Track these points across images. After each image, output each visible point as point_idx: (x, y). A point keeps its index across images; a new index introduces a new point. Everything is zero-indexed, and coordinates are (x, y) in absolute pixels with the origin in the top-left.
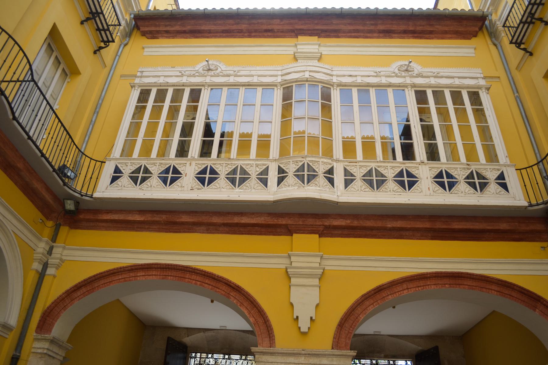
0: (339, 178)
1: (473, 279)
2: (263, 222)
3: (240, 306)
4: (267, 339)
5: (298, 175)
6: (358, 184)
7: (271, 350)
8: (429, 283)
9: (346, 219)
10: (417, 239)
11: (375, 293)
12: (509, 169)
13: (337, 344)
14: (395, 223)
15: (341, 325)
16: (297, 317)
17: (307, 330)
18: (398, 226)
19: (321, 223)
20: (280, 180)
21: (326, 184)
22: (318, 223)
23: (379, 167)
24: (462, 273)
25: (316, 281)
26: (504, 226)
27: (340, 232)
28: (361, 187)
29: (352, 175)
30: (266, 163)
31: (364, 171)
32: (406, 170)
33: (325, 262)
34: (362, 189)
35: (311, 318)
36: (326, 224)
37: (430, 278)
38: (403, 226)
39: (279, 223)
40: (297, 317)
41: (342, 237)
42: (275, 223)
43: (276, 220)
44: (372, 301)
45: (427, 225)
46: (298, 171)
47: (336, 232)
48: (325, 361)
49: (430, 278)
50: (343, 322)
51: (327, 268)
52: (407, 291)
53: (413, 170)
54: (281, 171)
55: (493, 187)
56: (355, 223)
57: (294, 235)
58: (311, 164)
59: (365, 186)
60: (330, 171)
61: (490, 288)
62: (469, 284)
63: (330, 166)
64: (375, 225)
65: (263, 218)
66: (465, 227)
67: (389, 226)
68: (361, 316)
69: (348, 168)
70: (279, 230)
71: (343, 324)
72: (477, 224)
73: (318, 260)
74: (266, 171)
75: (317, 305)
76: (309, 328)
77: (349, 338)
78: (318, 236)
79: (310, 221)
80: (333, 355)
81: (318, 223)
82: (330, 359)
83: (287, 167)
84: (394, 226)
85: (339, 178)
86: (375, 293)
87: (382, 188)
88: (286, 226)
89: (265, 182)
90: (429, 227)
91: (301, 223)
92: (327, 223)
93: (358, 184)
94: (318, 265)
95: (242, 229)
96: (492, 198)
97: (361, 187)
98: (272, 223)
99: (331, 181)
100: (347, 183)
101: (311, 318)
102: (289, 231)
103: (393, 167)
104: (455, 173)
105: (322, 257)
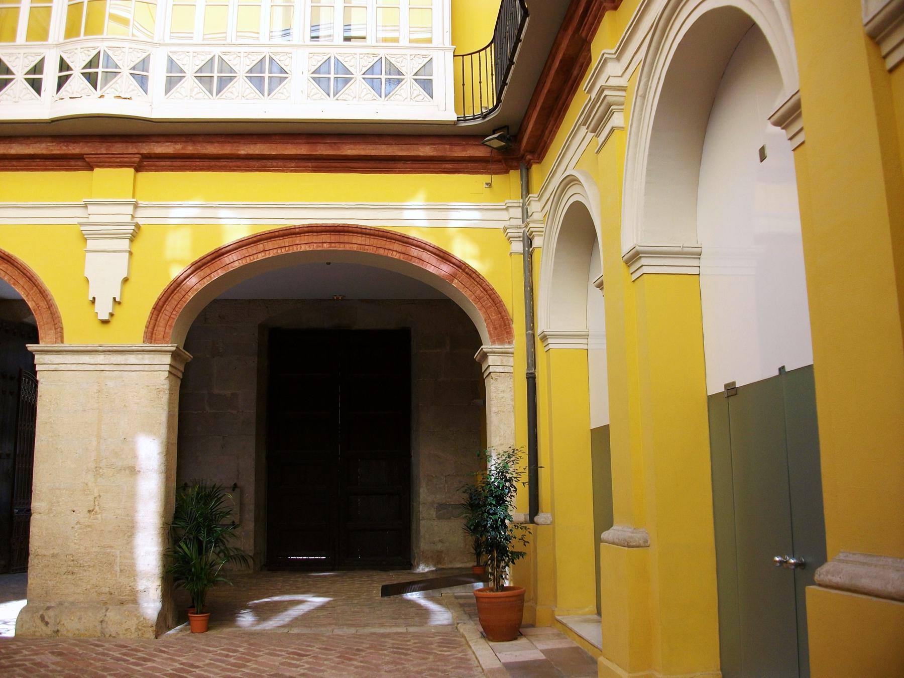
0: (157, 75)
1: (366, 234)
2: (44, 152)
3: (14, 284)
4: (53, 331)
5: (90, 73)
6: (189, 83)
7: (58, 346)
8: (298, 242)
9: (176, 143)
10: (291, 171)
11: (213, 259)
12: (441, 53)
13: (150, 335)
14: (252, 147)
15: (158, 309)
16: (94, 298)
17: (106, 317)
18: (257, 152)
19: (135, 151)
20: (62, 82)
21: (132, 87)
22: (131, 149)
23: (225, 53)
24: (349, 226)
25: (125, 244)
26: (426, 150)
27: (168, 163)
28: (192, 90)
29: (182, 71)
30: (41, 50)
31: (200, 61)
32: (271, 59)
33: (140, 213)
34: (194, 93)
35: (114, 299)
36: (144, 151)
37: (299, 233)
38: (264, 152)
39: (70, 152)
40: (94, 298)
41: (173, 170)
42: (62, 152)
43: (64, 148)
44: (209, 272)
45: (302, 150)
46: (90, 65)
47: (163, 163)
48: (132, 359)
49: (299, 233)
50: (161, 303)
51: (140, 221)
52: (263, 254)
53: (282, 59)
54: (64, 66)
55: (409, 87)
56: (190, 149)
57: (96, 170)
58: (110, 53)
59: (198, 86)
60: (144, 64)
61: (391, 247)
62: (359, 242)
63: (144, 55)
64: (221, 152)
65: (44, 145)
66: (363, 153)
67: (243, 152)
68: (190, 294)
69: (174, 57)
70: (72, 163)
71: (162, 307)
72: (384, 147)
73: (130, 209)
74: (38, 68)
75: (126, 280)
76: (112, 315)
77: (170, 326)
78: (132, 170)
79: (118, 148)
80: (143, 351)
81: (130, 151)
82: (140, 356)
83: (71, 60)
84: (251, 152)
85: (157, 75)
86: (213, 259)
87: (226, 92)
88: (80, 157)
89: (36, 85)
90: (305, 153)
91: (104, 152)
92: (146, 149)
93: (189, 83)
94: (128, 219)
95: (15, 163)
96: (406, 107)
97: (192, 90)
98: (58, 152)
99: (142, 81)
100: (171, 83)
101: (114, 299)
102: (86, 164)
103: (249, 53)
104: (351, 64)
105: (136, 206)
